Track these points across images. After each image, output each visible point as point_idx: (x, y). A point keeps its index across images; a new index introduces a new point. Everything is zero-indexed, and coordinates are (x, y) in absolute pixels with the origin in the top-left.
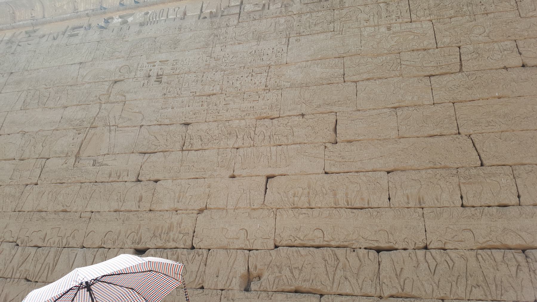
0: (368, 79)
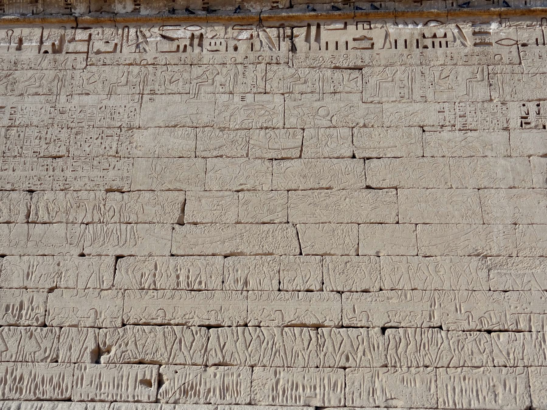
0: (217, 157)
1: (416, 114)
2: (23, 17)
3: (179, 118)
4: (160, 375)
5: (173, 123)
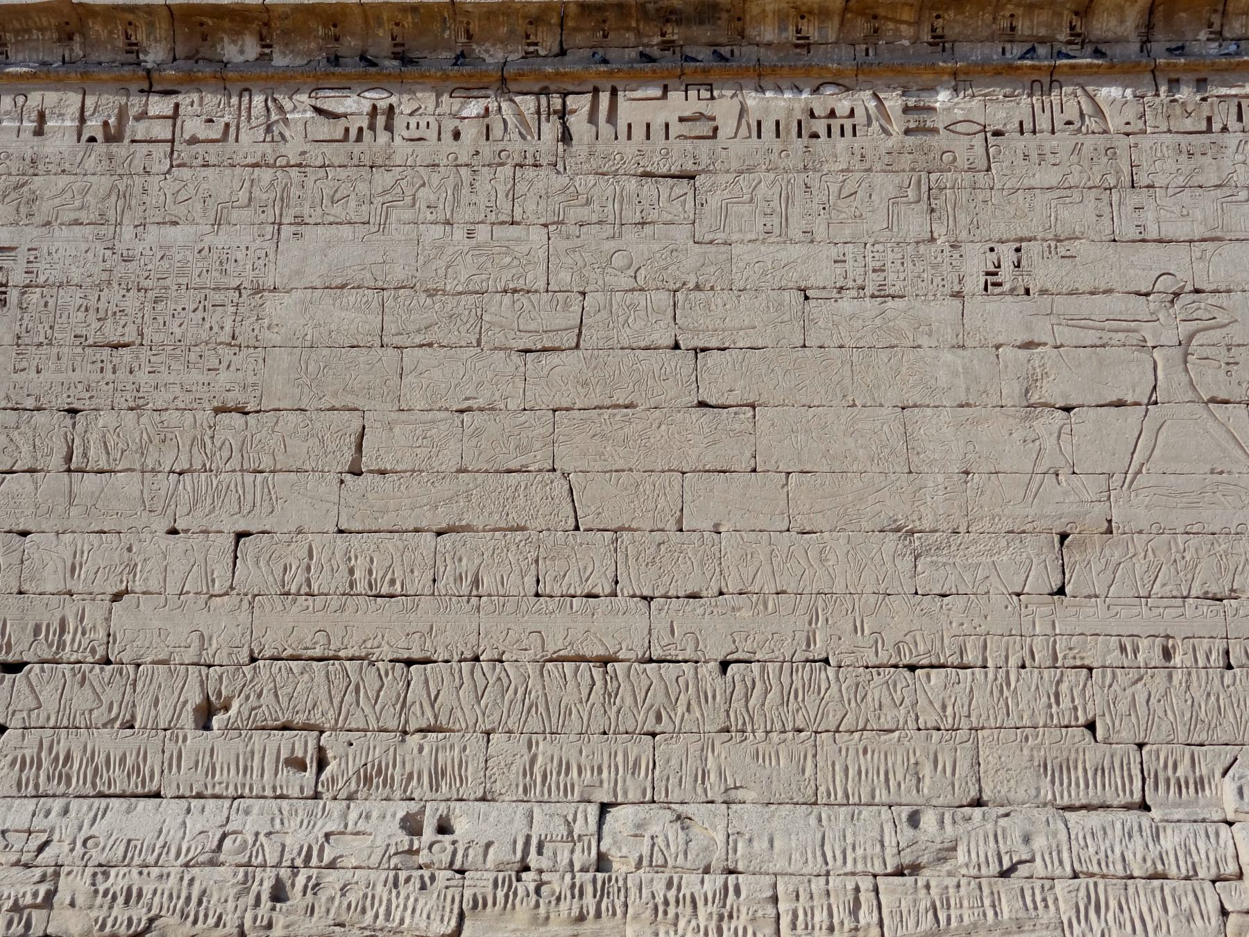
0: (421, 346)
2: (45, 69)
3: (350, 271)
4: (321, 750)
5: (339, 281)
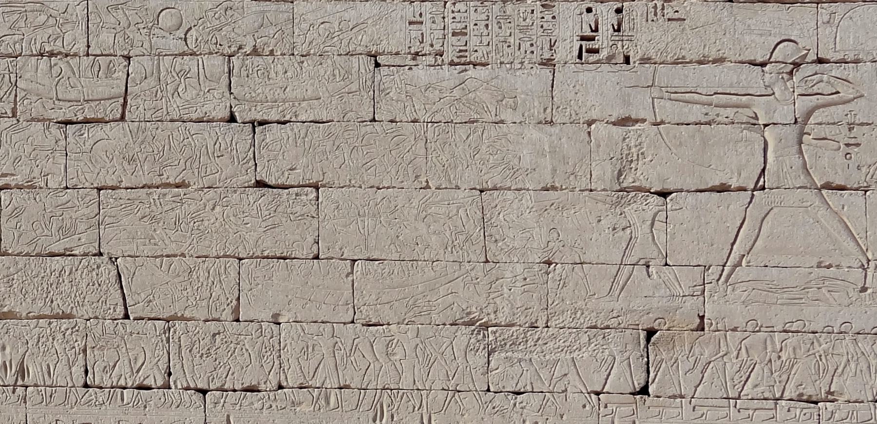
1: (362, 26)
